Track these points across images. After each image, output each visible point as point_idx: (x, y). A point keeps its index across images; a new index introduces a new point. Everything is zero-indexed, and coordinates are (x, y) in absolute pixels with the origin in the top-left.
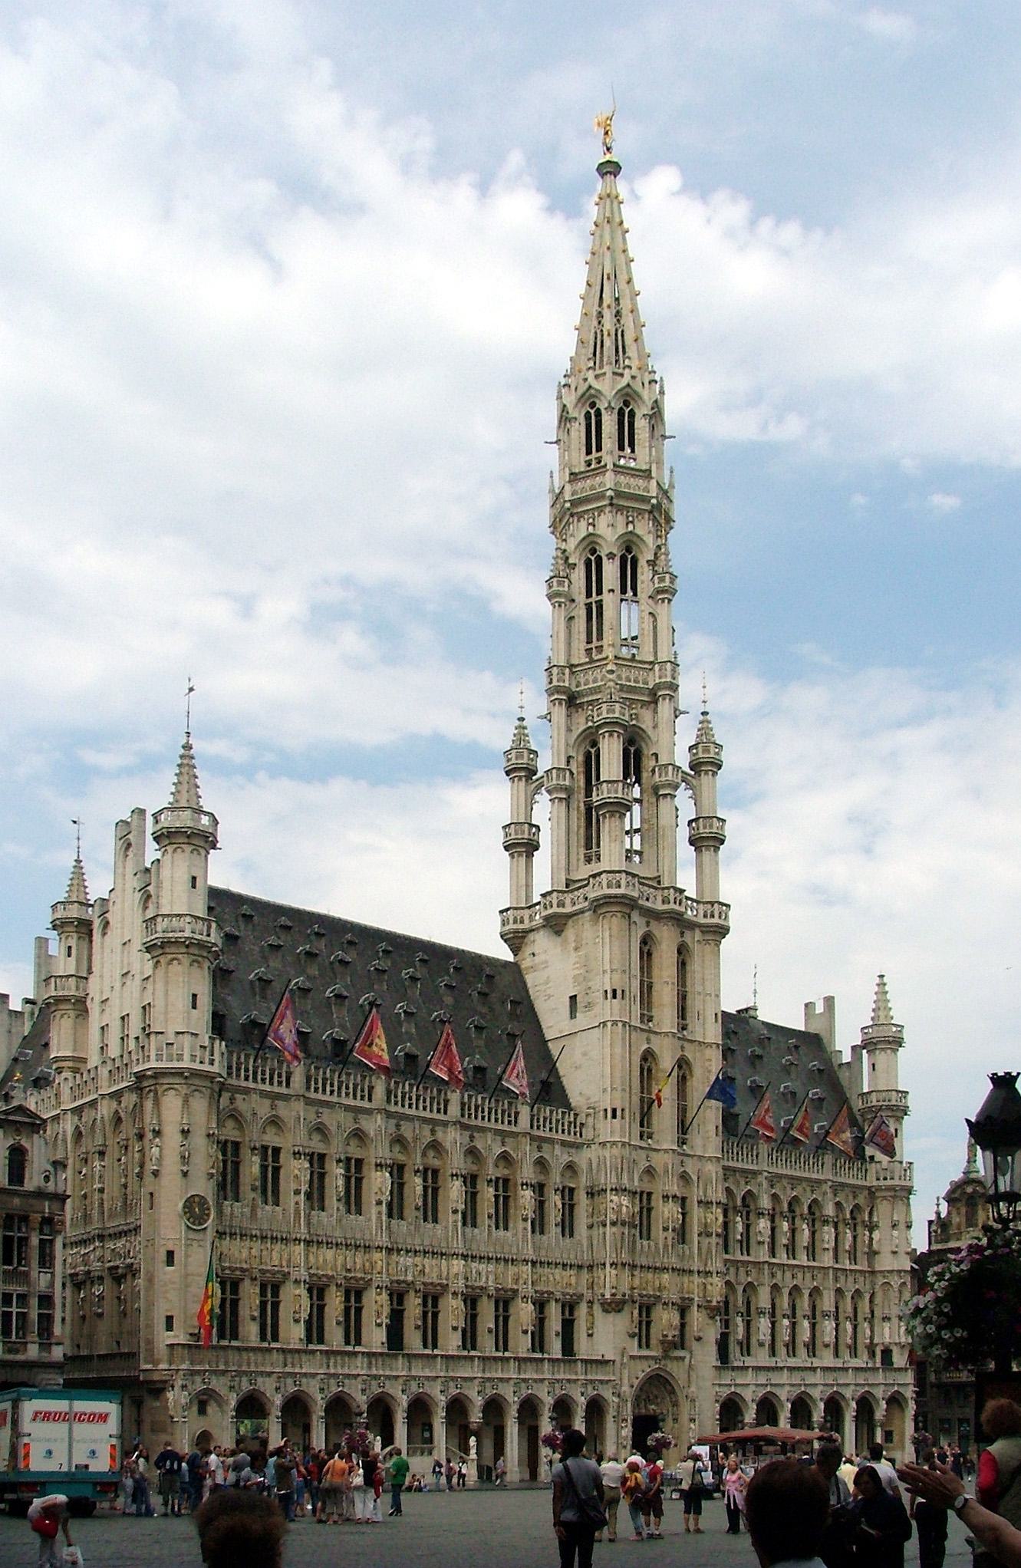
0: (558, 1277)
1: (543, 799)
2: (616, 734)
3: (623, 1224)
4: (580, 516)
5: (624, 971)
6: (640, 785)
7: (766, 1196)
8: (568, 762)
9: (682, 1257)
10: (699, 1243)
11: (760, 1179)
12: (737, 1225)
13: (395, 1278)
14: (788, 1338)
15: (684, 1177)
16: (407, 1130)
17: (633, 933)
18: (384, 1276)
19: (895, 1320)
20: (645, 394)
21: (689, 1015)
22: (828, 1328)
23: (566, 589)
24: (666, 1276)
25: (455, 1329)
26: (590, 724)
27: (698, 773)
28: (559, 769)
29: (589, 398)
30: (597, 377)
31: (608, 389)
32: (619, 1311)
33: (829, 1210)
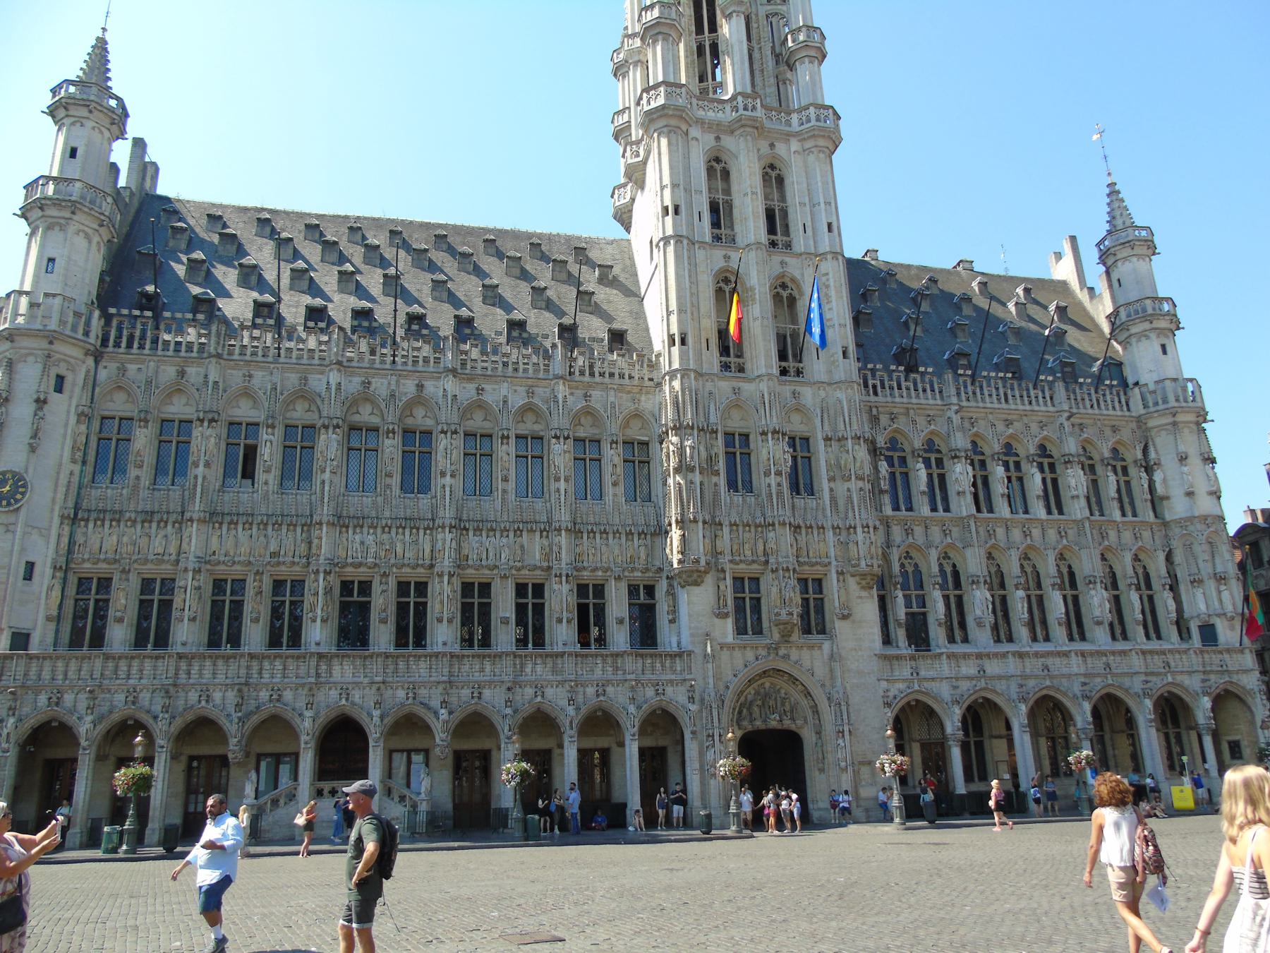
0: (616, 552)
3: (691, 469)
7: (959, 435)
10: (831, 490)
11: (949, 414)
12: (919, 473)
13: (350, 560)
14: (1026, 615)
15: (799, 409)
16: (381, 386)
18: (322, 558)
19: (1211, 585)
21: (792, 229)
22: (1096, 601)
24: (772, 534)
25: (440, 620)
32: (696, 583)
33: (1072, 446)
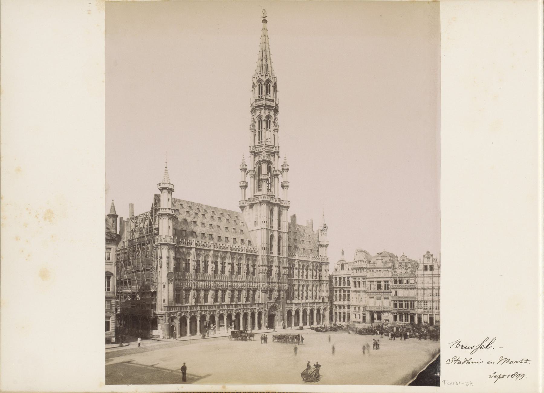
1: (248, 176)
2: (265, 163)
4: (257, 110)
5: (267, 217)
6: (270, 173)
8: (254, 169)
9: (279, 279)
17: (269, 208)
20: (273, 80)
23: (254, 128)
26: (259, 160)
27: (284, 171)
28: (252, 170)
29: (260, 81)
30: (261, 76)
31: (264, 79)
33: (311, 267)
